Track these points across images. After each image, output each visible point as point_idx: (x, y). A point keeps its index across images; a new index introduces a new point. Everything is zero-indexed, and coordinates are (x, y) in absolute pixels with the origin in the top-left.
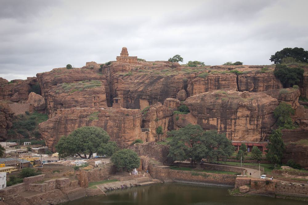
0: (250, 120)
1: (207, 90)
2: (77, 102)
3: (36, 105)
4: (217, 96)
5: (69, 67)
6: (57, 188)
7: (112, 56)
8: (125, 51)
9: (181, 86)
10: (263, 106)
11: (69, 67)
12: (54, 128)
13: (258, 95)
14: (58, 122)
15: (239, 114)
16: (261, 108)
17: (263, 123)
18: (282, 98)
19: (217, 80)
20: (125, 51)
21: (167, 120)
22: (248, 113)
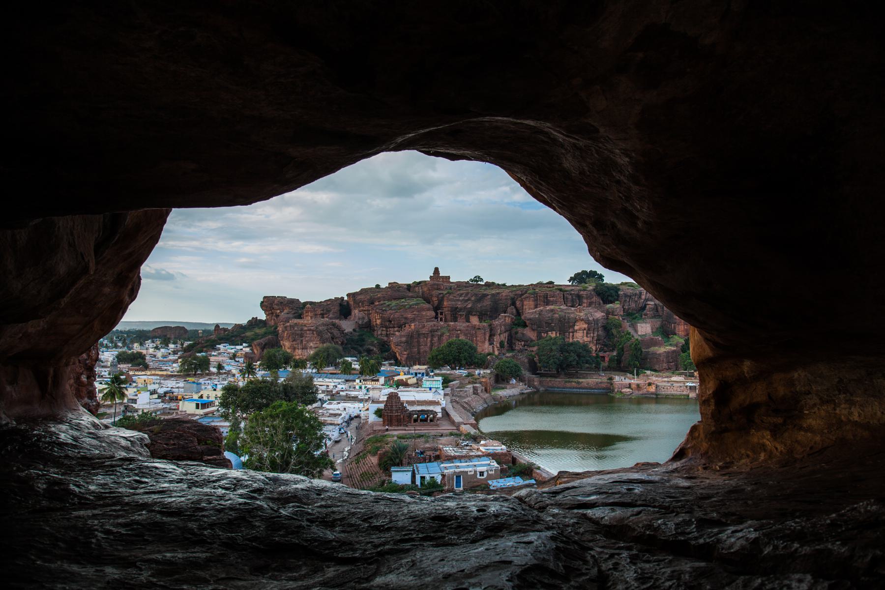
0: (587, 333)
1: (536, 307)
2: (406, 318)
3: (360, 322)
4: (552, 310)
5: (378, 286)
6: (474, 393)
7: (425, 276)
8: (436, 270)
9: (510, 302)
10: (597, 320)
11: (378, 286)
12: (407, 342)
13: (590, 310)
14: (410, 336)
15: (576, 328)
16: (596, 321)
17: (598, 335)
18: (608, 313)
19: (546, 296)
20: (436, 270)
21: (506, 335)
22: (586, 326)
